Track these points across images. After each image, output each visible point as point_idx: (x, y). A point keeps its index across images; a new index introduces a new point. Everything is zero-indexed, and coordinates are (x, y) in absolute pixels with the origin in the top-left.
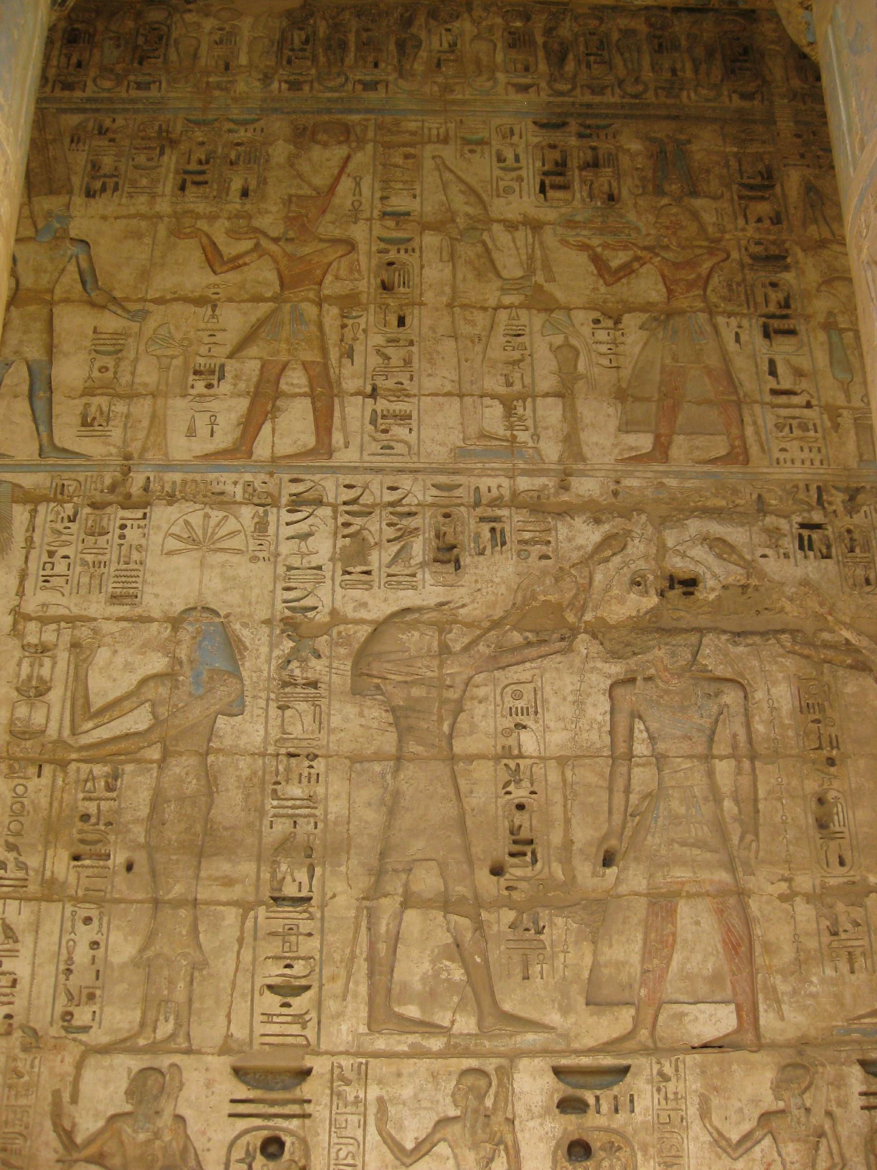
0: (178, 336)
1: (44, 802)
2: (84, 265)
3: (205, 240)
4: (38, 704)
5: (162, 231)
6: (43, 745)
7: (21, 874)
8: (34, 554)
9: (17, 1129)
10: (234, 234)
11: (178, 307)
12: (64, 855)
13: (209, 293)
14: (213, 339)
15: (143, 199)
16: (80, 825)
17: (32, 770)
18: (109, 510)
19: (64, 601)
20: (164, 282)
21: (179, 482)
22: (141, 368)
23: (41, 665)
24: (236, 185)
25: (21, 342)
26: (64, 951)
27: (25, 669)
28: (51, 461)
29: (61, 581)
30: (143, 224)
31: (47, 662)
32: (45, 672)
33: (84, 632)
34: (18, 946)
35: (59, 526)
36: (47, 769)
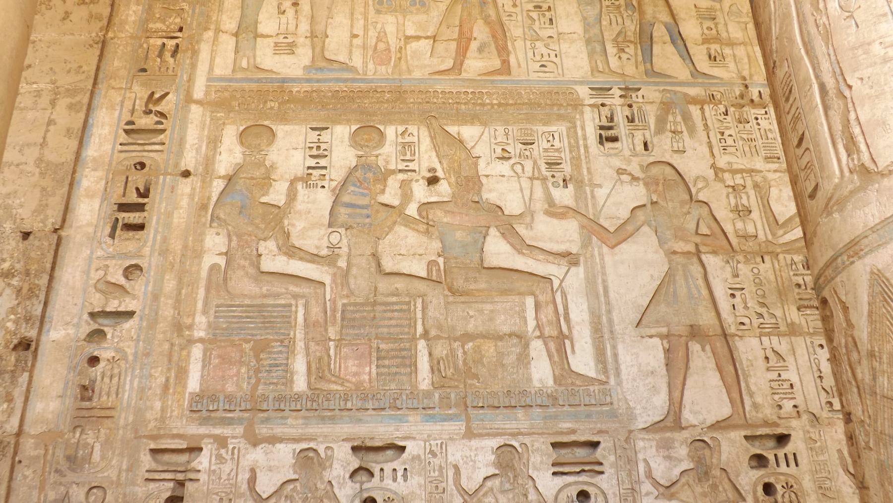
1: (772, 278)
4: (748, 221)
7: (774, 321)
8: (712, 134)
9: (824, 475)
12: (794, 309)
16: (797, 290)
17: (759, 259)
22: (730, 29)
23: (741, 198)
25: (654, 12)
26: (814, 365)
27: (733, 201)
29: (733, 149)
31: (744, 196)
32: (744, 201)
34: (786, 364)
36: (767, 258)
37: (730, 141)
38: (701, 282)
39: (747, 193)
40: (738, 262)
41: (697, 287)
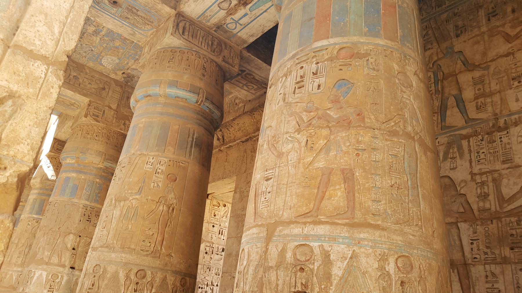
0: (503, 69)
2: (463, 59)
3: (503, 34)
5: (486, 37)
6: (491, 214)
8: (472, 154)
10: (513, 27)
11: (499, 60)
13: (510, 51)
14: (516, 66)
15: (476, 30)
18: (494, 134)
19: (486, 167)
20: (492, 54)
21: (517, 118)
23: (484, 188)
24: (509, 9)
27: (479, 191)
28: (470, 124)
29: (484, 160)
30: (479, 38)
31: (486, 187)
32: (486, 190)
33: (496, 175)
35: (478, 143)
37: (482, 156)
38: (456, 238)
39: (488, 186)
40: (477, 225)
41: (454, 240)
